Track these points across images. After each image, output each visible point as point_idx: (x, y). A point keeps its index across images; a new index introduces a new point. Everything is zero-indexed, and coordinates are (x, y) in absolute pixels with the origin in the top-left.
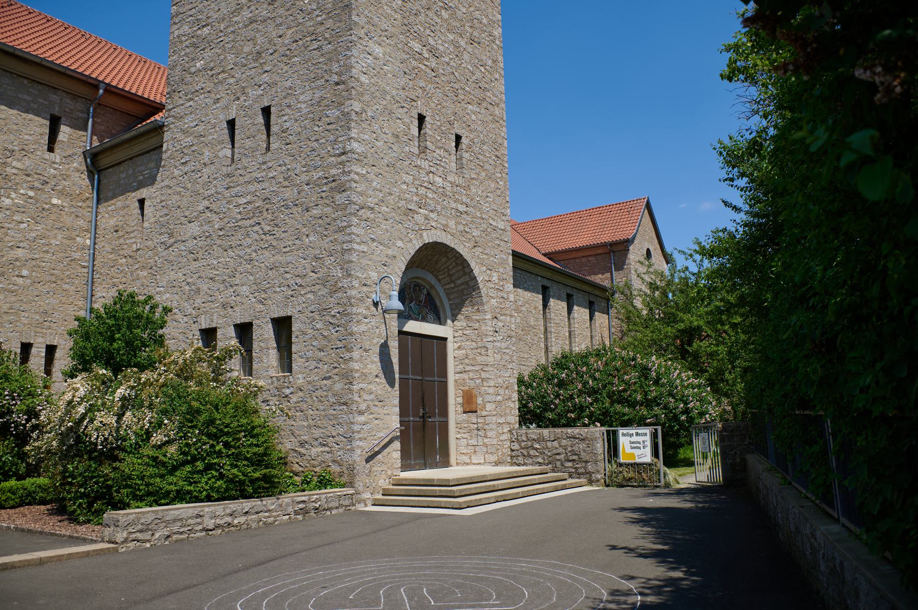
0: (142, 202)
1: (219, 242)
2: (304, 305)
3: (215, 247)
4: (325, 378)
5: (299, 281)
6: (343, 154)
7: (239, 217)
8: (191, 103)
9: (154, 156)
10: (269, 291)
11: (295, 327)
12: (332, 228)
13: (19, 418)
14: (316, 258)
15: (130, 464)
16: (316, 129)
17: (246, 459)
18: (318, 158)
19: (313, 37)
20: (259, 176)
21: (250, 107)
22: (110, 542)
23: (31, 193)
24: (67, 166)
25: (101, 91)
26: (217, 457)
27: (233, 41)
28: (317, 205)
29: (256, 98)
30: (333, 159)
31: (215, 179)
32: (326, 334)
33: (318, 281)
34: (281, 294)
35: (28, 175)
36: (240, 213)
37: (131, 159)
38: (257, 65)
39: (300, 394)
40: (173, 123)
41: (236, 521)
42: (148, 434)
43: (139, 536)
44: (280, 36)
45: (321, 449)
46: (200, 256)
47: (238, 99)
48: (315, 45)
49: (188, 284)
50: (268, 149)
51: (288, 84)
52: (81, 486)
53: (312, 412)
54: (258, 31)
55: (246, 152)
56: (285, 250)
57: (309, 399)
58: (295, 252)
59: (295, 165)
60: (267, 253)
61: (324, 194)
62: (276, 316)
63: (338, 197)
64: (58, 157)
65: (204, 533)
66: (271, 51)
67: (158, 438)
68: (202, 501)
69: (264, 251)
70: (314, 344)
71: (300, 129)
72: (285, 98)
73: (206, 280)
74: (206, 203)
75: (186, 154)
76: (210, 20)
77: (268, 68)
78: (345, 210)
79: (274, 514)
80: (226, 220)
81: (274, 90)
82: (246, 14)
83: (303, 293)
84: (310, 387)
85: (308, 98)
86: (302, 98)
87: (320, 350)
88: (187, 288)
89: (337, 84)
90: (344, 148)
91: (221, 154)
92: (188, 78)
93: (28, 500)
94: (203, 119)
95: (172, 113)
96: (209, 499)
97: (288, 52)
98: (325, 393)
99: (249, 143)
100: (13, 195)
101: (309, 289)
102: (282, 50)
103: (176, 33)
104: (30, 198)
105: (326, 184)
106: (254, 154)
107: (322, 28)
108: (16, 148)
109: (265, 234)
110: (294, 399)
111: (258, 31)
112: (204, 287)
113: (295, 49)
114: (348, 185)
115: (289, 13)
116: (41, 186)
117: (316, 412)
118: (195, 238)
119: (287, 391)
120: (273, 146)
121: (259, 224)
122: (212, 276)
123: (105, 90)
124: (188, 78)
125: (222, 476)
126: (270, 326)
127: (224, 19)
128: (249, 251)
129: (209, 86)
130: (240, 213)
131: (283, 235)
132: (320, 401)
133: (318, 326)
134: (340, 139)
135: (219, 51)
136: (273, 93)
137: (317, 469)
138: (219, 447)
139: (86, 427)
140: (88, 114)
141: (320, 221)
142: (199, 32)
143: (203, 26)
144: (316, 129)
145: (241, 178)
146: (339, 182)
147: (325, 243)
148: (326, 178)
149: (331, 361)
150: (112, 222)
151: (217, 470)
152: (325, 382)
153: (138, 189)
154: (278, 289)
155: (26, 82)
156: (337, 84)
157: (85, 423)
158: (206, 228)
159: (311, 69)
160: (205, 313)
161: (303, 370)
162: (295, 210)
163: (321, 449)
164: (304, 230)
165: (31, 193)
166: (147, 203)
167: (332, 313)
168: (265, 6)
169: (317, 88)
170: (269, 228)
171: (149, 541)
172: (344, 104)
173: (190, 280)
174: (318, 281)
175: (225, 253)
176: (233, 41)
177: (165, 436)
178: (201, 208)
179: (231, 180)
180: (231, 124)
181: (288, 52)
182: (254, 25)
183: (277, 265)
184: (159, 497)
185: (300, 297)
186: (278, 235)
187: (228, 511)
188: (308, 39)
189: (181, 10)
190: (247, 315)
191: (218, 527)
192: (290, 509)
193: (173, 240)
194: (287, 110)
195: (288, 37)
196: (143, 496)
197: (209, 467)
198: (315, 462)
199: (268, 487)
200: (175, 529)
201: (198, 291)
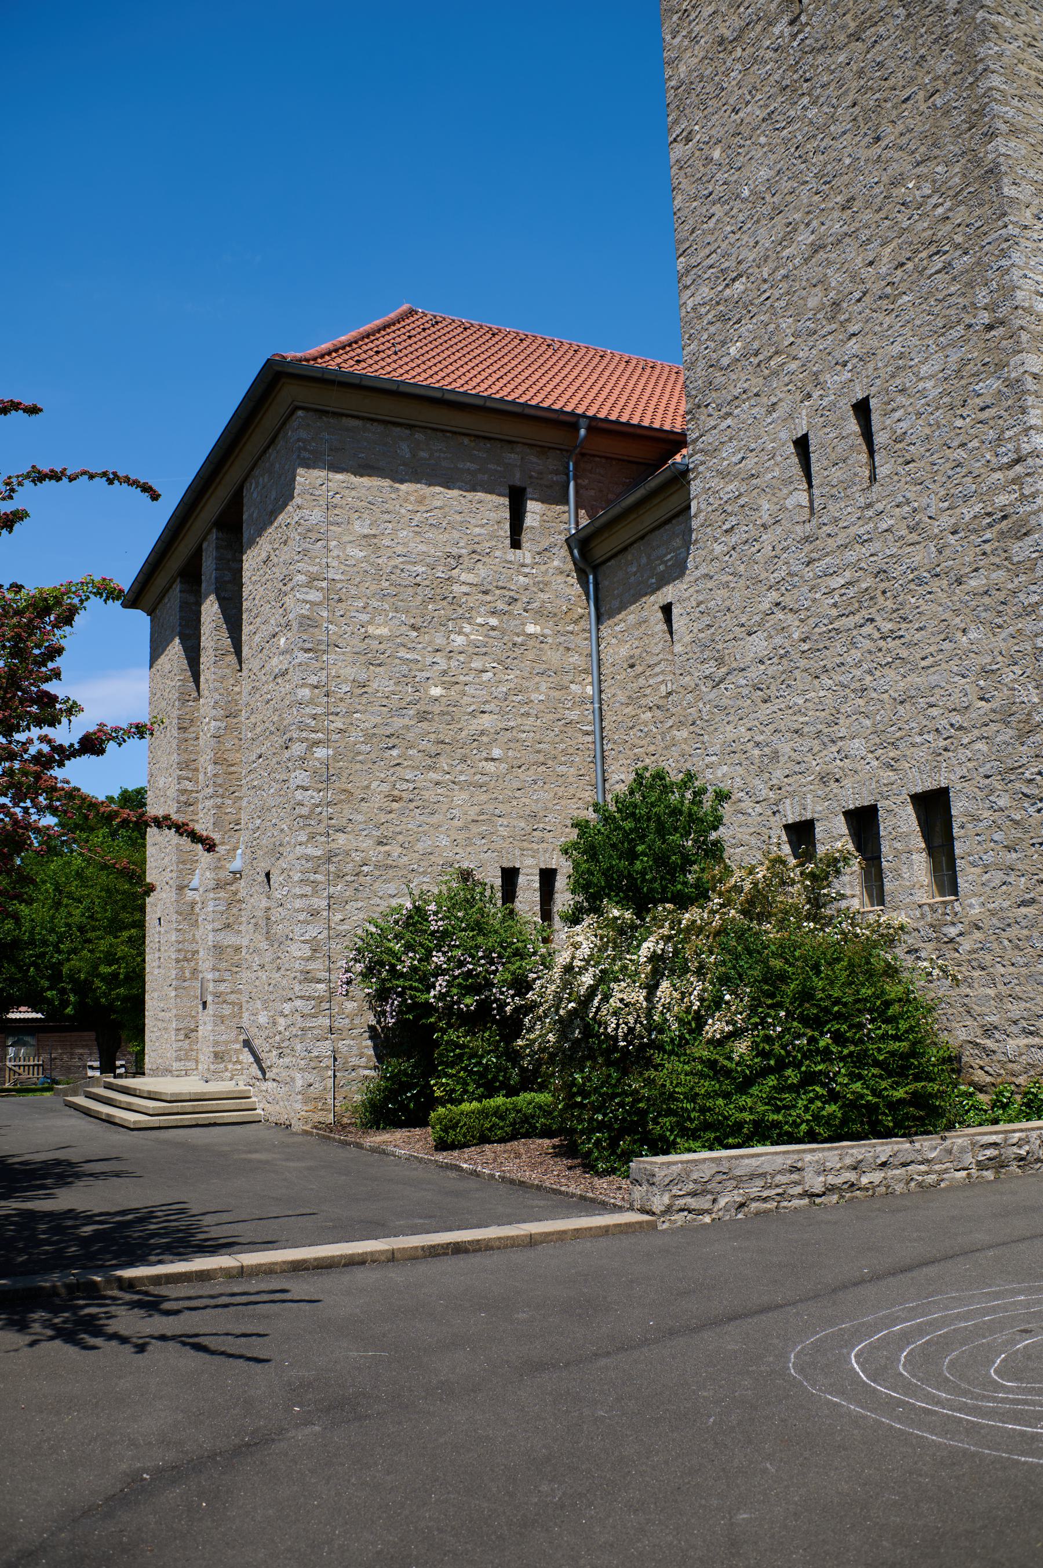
0: (667, 610)
1: (803, 663)
2: (970, 765)
3: (797, 672)
4: (1024, 903)
5: (956, 719)
6: (1018, 461)
7: (834, 612)
8: (729, 421)
9: (677, 526)
10: (902, 744)
11: (958, 807)
12: (1010, 610)
13: (502, 993)
14: (986, 672)
15: (672, 1073)
16: (959, 423)
17: (877, 1064)
18: (969, 479)
19: (933, 249)
20: (862, 531)
21: (832, 407)
22: (643, 1211)
23: (493, 621)
24: (543, 568)
25: (583, 432)
26: (823, 1061)
27: (788, 293)
28: (976, 570)
29: (841, 386)
30: (998, 475)
31: (785, 549)
32: (1018, 817)
33: (993, 716)
34: (924, 748)
35: (486, 593)
36: (835, 605)
37: (642, 538)
38: (834, 326)
39: (978, 935)
40: (703, 463)
41: (864, 1180)
42: (700, 1021)
43: (692, 1202)
44: (871, 263)
45: (1026, 1041)
46: (773, 692)
47: (809, 396)
48: (938, 263)
49: (758, 744)
50: (873, 478)
51: (897, 348)
52: (597, 1111)
53: (1002, 970)
54: (829, 263)
55: (834, 491)
56: (924, 663)
57: (995, 945)
58: (944, 666)
59: (925, 501)
60: (891, 673)
61: (987, 547)
62: (919, 789)
63: (1015, 547)
64: (528, 555)
65: (806, 1201)
66: (857, 295)
67: (715, 1027)
68: (800, 1141)
69: (886, 671)
70: (996, 837)
71: (927, 431)
72: (893, 376)
73: (788, 735)
74: (774, 596)
75: (730, 514)
76: (744, 266)
77: (855, 329)
78: (1033, 570)
79: (937, 1167)
80: (812, 621)
81: (871, 366)
82: (805, 237)
83: (965, 741)
84: (995, 921)
85: (937, 368)
86: (924, 370)
87: (1009, 849)
88: (757, 752)
89: (990, 327)
90: (1017, 450)
91: (790, 503)
92: (719, 379)
93: (522, 1128)
94: (753, 446)
95: (700, 445)
96: (812, 1137)
97: (888, 290)
98: (1025, 932)
99: (836, 474)
100: (467, 628)
101: (976, 733)
102: (876, 288)
103: (690, 304)
104: (493, 628)
105: (990, 526)
106: (849, 492)
107: (948, 227)
108: (464, 551)
109: (883, 638)
110: (966, 944)
111: (829, 263)
112: (785, 749)
113: (902, 280)
114: (1033, 522)
115: (882, 214)
116: (506, 608)
117: (1011, 969)
118: (761, 662)
119: (952, 931)
120: (882, 471)
121: (872, 620)
122: (796, 726)
123: (589, 429)
124: (719, 379)
125: (833, 1097)
126: (910, 809)
127: (766, 258)
128: (858, 673)
129: (756, 383)
130: (835, 605)
131: (918, 636)
132: (1017, 947)
133: (1002, 803)
134: (1008, 434)
135: (765, 318)
136: (870, 371)
137: (1021, 1080)
138: (825, 1041)
139: (598, 1009)
140: (567, 475)
141: (986, 600)
142: (728, 292)
143: (734, 280)
144: (959, 423)
145: (830, 541)
146: (1015, 517)
147: (1000, 642)
148: (989, 514)
149: (1033, 869)
150: (624, 651)
151: (823, 1085)
152: (1024, 910)
153: (658, 589)
154: (919, 739)
155: (466, 441)
156: (990, 327)
157: (596, 1003)
158: (778, 640)
159: (936, 310)
160: (792, 795)
161: (977, 889)
162: (935, 584)
163: (1026, 1041)
164: (958, 620)
165: (493, 621)
166: (675, 611)
167: (1027, 775)
168: (836, 214)
169: (952, 344)
170: (890, 626)
171: (708, 1212)
172: (1007, 365)
173: (760, 738)
174: (993, 716)
175: (816, 682)
176: (788, 293)
177: (728, 1023)
178: (766, 606)
179: (812, 547)
180: (802, 445)
181: (888, 290)
182: (822, 255)
183: (913, 693)
184: (725, 1134)
185: (961, 750)
186: (908, 638)
187: (848, 1161)
188: (924, 255)
189: (693, 261)
190: (865, 792)
191: (830, 1189)
192: (968, 1159)
193: (724, 670)
194: (901, 399)
195: (885, 260)
196: (696, 1130)
197: (809, 1079)
198: (1015, 1067)
199: (923, 1116)
200: (754, 1191)
201: (775, 756)
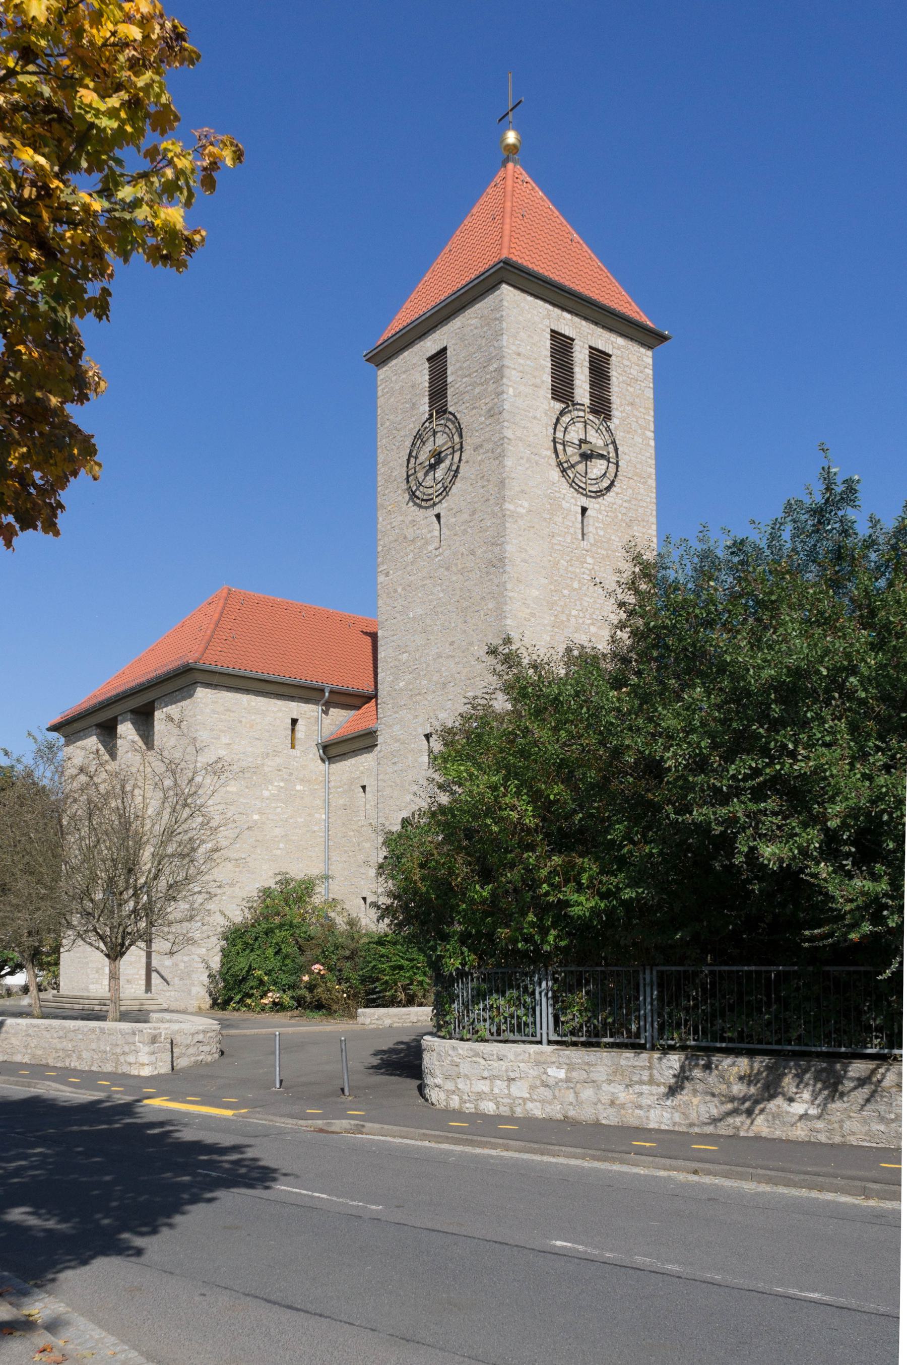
8: (397, 715)
23: (282, 784)
35: (279, 770)
64: (298, 752)
77: (451, 697)
100: (270, 787)
104: (282, 788)
116: (288, 778)
150: (341, 802)
165: (282, 784)
182: (441, 660)
